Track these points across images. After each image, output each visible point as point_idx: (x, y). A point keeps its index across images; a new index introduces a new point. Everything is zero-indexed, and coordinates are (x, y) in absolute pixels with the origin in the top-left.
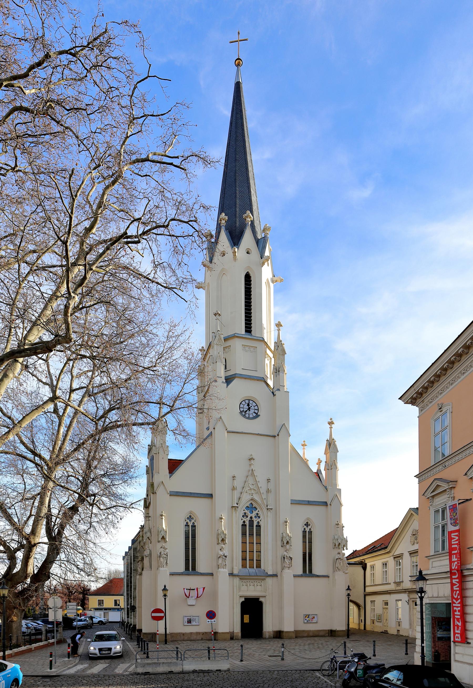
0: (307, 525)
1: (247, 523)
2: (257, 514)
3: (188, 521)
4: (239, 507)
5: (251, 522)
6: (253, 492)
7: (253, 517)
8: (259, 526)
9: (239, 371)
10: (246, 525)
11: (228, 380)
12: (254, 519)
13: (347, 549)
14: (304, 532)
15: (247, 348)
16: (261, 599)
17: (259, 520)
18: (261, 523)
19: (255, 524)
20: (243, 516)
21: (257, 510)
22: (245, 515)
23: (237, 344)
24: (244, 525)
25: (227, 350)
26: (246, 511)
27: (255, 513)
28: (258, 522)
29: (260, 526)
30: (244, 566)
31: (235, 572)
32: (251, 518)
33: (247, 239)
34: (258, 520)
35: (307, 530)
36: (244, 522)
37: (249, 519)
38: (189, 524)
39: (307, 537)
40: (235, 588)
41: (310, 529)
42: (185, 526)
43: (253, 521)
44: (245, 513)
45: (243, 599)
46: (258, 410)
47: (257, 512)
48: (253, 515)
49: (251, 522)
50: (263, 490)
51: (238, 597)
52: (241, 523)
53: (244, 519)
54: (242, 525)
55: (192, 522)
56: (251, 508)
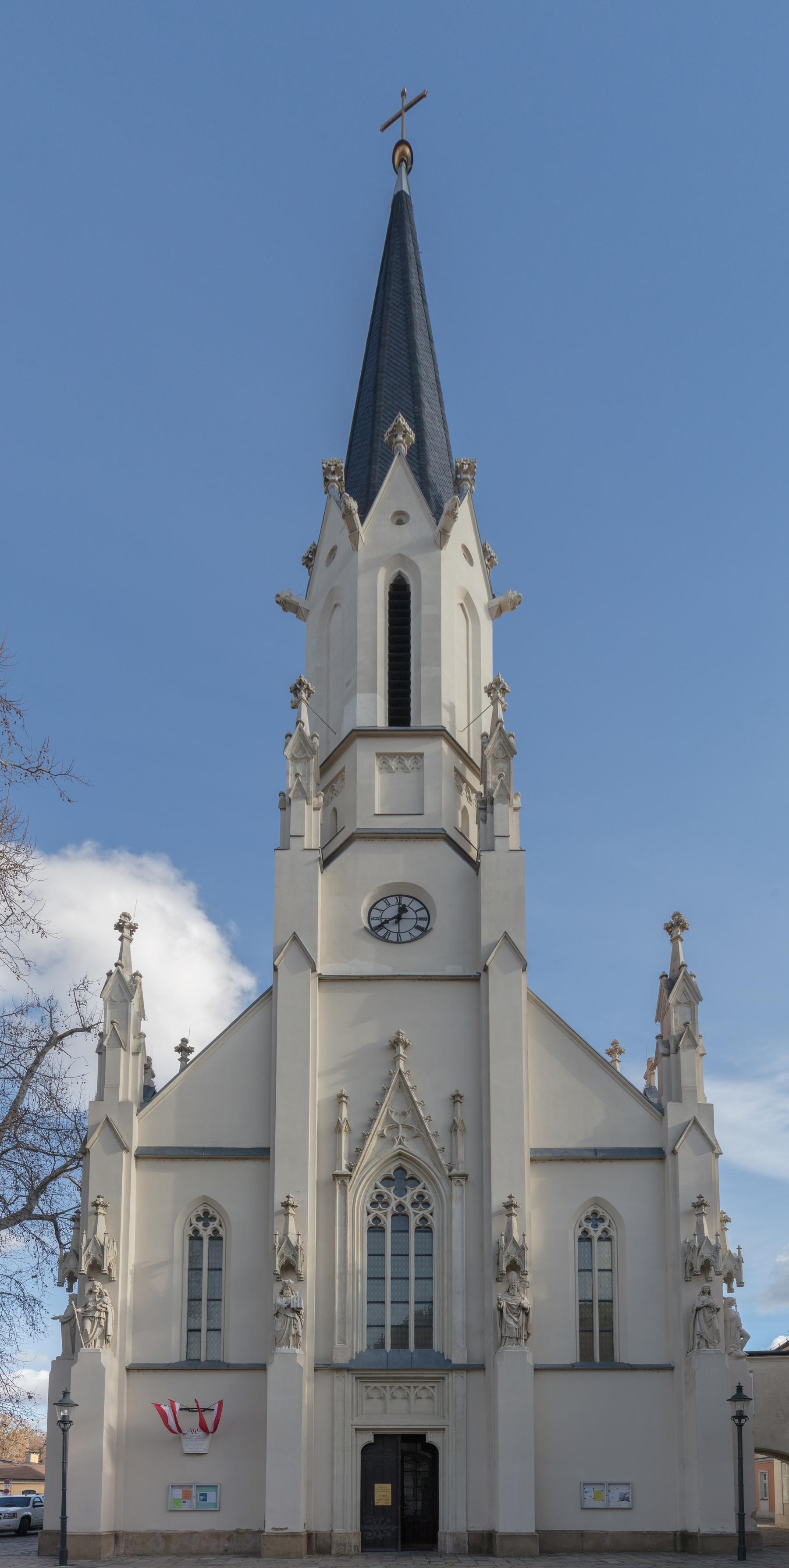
2: (421, 1196)
5: (401, 1215)
7: (408, 1204)
10: (382, 1230)
12: (411, 1210)
19: (414, 1221)
20: (374, 1204)
21: (421, 1185)
22: (379, 1201)
24: (376, 1229)
26: (383, 1189)
29: (429, 1230)
32: (400, 1206)
36: (377, 1219)
43: (406, 1216)
44: (380, 1196)
47: (418, 1189)
48: (407, 1200)
49: (401, 1215)
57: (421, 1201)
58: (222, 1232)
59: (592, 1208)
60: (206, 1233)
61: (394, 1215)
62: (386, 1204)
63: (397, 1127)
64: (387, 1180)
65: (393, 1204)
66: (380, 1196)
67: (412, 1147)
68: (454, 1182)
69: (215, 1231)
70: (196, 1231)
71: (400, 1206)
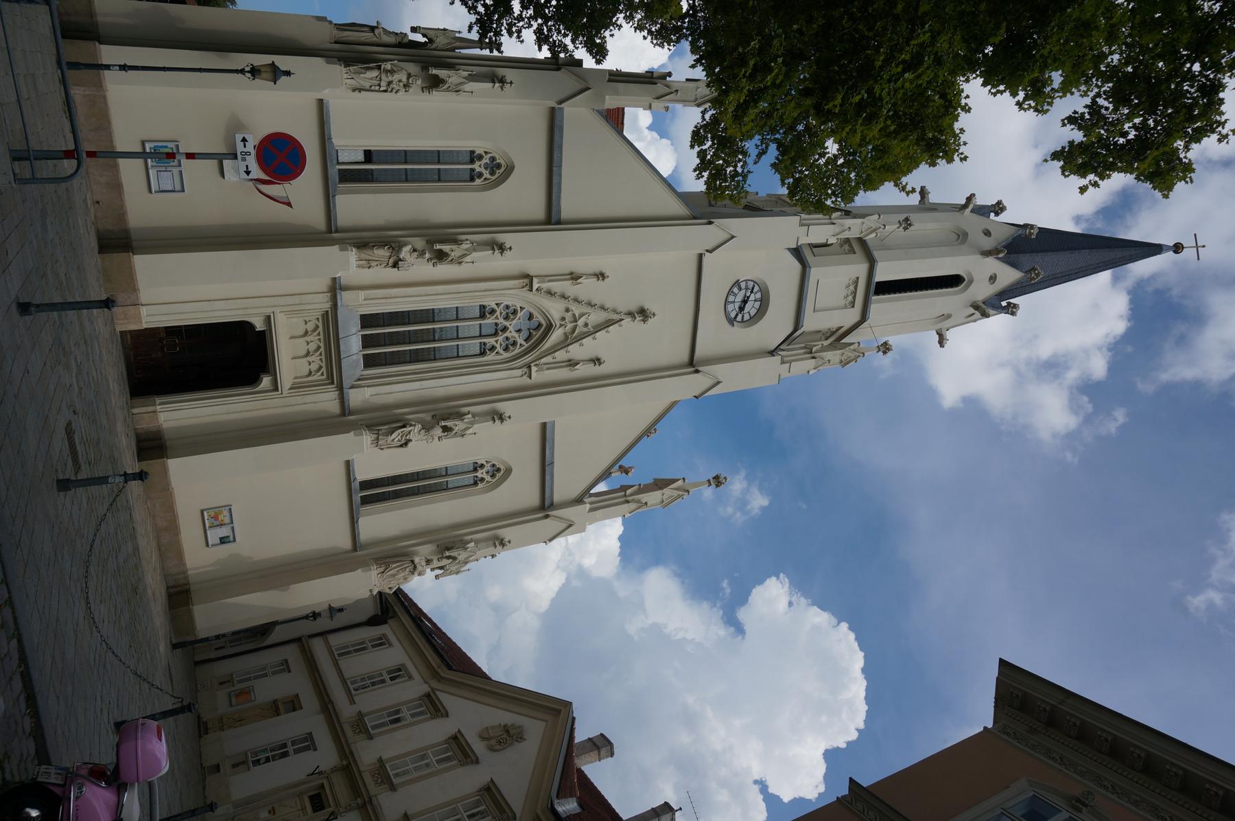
2: (514, 343)
3: (486, 160)
4: (530, 296)
6: (570, 326)
7: (507, 334)
9: (814, 273)
11: (797, 252)
12: (501, 338)
13: (437, 577)
15: (852, 288)
16: (266, 381)
17: (499, 349)
18: (490, 357)
19: (490, 341)
20: (507, 307)
22: (511, 313)
23: (861, 269)
25: (846, 247)
28: (493, 348)
30: (368, 321)
31: (345, 298)
32: (505, 329)
33: (1009, 275)
36: (493, 312)
38: (478, 163)
40: (296, 300)
41: (482, 480)
42: (472, 152)
43: (496, 334)
45: (259, 326)
46: (742, 321)
50: (575, 351)
51: (268, 311)
54: (483, 307)
55: (484, 171)
58: (478, 182)
59: (502, 468)
60: (477, 166)
61: (496, 324)
63: (575, 321)
65: (507, 323)
66: (515, 312)
67: (556, 336)
68: (525, 369)
69: (480, 175)
70: (480, 157)
71: (505, 329)
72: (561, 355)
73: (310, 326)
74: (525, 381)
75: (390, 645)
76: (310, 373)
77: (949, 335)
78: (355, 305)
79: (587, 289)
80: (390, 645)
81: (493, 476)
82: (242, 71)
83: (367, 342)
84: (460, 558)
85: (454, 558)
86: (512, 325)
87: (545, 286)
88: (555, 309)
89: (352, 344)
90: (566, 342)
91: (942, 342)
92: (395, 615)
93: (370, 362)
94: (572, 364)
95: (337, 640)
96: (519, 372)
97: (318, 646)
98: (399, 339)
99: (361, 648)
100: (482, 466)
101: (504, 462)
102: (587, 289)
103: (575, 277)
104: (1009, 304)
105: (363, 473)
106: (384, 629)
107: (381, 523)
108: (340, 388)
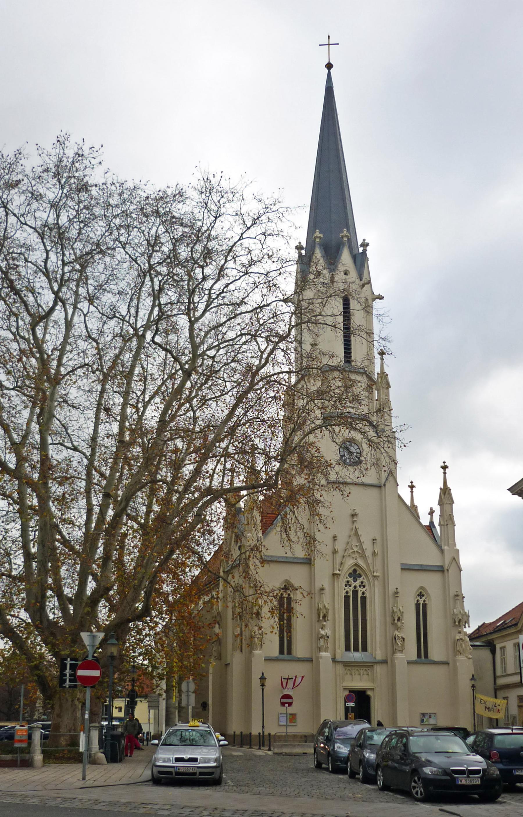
0: (421, 595)
1: (351, 594)
2: (362, 582)
4: (342, 575)
5: (355, 592)
6: (357, 555)
7: (358, 585)
8: (364, 598)
10: (349, 597)
13: (469, 627)
14: (418, 605)
16: (369, 693)
17: (364, 590)
18: (367, 594)
19: (360, 595)
20: (346, 586)
22: (348, 584)
24: (347, 598)
26: (349, 579)
27: (359, 580)
28: (363, 593)
30: (347, 649)
32: (355, 587)
34: (363, 590)
35: (421, 602)
36: (347, 592)
37: (352, 588)
39: (422, 612)
41: (424, 601)
43: (357, 591)
44: (348, 582)
45: (347, 693)
47: (361, 579)
48: (358, 583)
49: (355, 592)
50: (368, 553)
51: (342, 689)
52: (343, 593)
53: (347, 589)
54: (345, 597)
56: (355, 574)
57: (362, 585)
62: (350, 586)
64: (350, 575)
65: (353, 586)
67: (361, 563)
72: (370, 561)
73: (348, 672)
74: (380, 579)
75: (505, 647)
76: (368, 674)
77: (376, 293)
78: (341, 653)
79: (340, 546)
80: (505, 647)
81: (423, 596)
82: (263, 689)
83: (356, 649)
84: (460, 617)
85: (460, 620)
86: (354, 584)
87: (338, 567)
88: (349, 563)
89: (357, 656)
90: (363, 556)
91: (381, 298)
92: (493, 640)
93: (365, 649)
94: (374, 554)
95: (499, 673)
96: (376, 582)
97: (501, 681)
98: (356, 636)
99: (504, 661)
100: (418, 601)
101: (418, 590)
102: (340, 546)
103: (335, 552)
104: (362, 245)
105: (414, 656)
106: (498, 647)
107: (437, 650)
108: (376, 663)
